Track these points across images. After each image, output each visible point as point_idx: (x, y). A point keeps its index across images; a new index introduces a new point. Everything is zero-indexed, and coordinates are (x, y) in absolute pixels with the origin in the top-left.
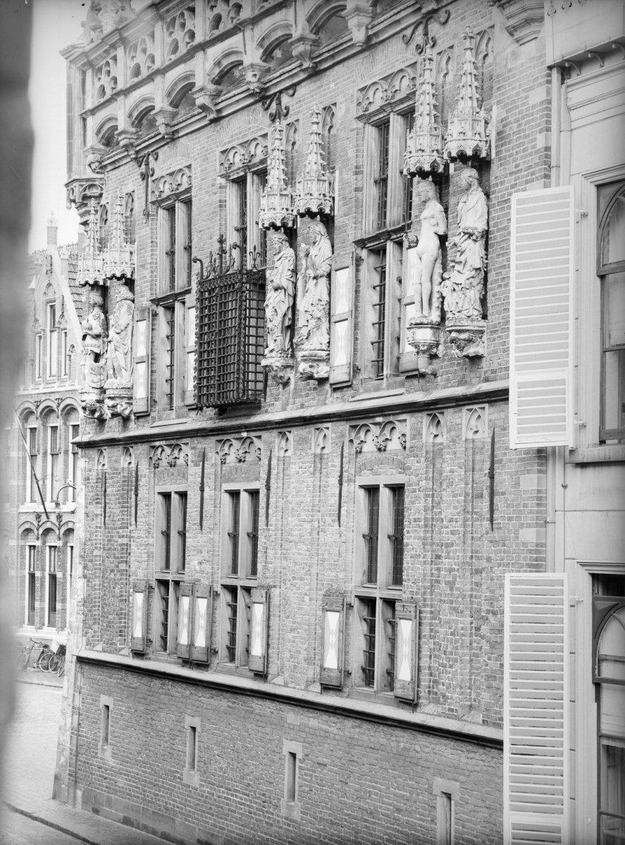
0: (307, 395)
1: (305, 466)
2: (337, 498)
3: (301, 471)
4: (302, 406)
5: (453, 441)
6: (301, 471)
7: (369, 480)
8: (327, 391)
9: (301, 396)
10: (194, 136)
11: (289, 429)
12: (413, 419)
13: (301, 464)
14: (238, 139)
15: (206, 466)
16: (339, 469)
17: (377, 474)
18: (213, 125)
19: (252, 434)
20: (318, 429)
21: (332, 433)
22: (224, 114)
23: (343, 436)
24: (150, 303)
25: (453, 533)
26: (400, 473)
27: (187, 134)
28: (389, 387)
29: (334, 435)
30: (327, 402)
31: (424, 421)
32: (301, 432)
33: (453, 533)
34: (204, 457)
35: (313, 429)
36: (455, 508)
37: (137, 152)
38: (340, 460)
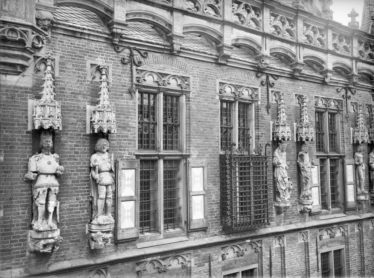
0: (293, 218)
1: (295, 250)
2: (316, 261)
3: (292, 253)
4: (290, 223)
5: (367, 231)
6: (292, 253)
7: (325, 250)
8: (306, 216)
9: (290, 219)
10: (193, 62)
11: (283, 235)
12: (351, 225)
13: (292, 250)
14: (236, 82)
15: (212, 264)
16: (316, 248)
17: (330, 247)
18: (214, 65)
19: (254, 240)
20: (300, 233)
21: (310, 232)
22: (229, 64)
23: (316, 234)
24: (134, 157)
25: (368, 261)
26: (341, 245)
27: (185, 57)
28: (333, 213)
29: (311, 234)
30: (306, 220)
31: (355, 225)
32: (291, 235)
33: (368, 261)
34: (209, 260)
35: (299, 233)
36: (369, 252)
37: (120, 41)
38: (315, 244)
